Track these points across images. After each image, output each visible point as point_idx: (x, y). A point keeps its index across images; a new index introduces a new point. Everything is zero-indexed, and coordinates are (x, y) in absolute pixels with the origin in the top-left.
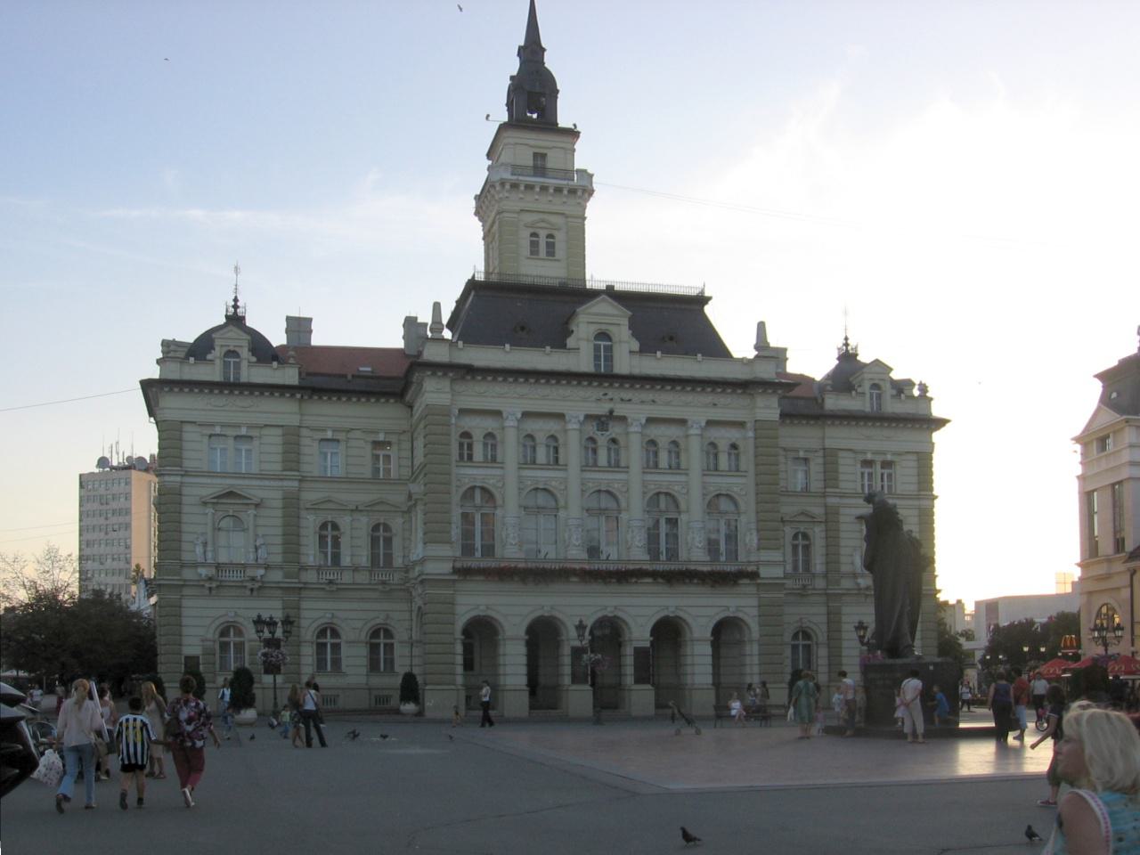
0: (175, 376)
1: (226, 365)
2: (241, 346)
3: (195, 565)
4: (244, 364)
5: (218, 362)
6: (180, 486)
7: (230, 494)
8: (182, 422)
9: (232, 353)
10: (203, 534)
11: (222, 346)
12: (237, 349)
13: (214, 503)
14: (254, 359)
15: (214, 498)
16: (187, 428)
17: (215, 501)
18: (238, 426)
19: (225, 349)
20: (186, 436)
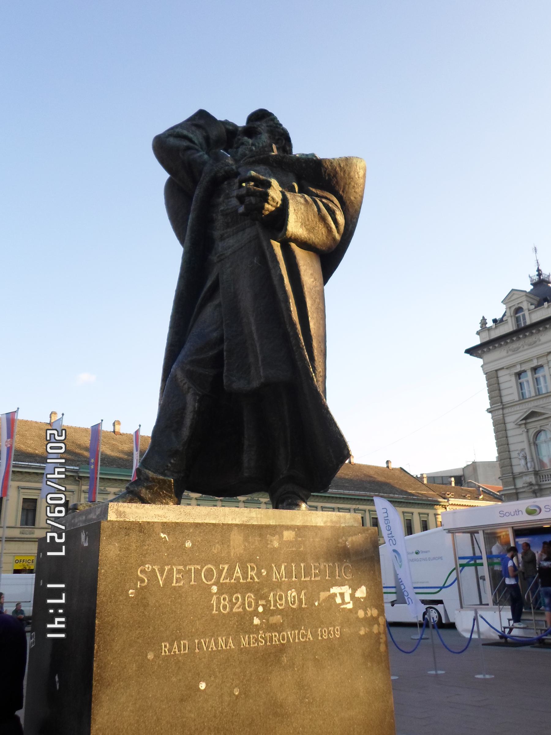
0: (487, 339)
1: (518, 320)
2: (522, 302)
3: (522, 474)
4: (526, 313)
5: (509, 320)
6: (503, 417)
7: (533, 414)
8: (496, 371)
9: (519, 310)
10: (523, 450)
11: (510, 308)
12: (520, 305)
13: (525, 424)
14: (533, 307)
15: (522, 420)
16: (500, 373)
17: (524, 422)
18: (530, 360)
19: (513, 309)
20: (501, 380)
